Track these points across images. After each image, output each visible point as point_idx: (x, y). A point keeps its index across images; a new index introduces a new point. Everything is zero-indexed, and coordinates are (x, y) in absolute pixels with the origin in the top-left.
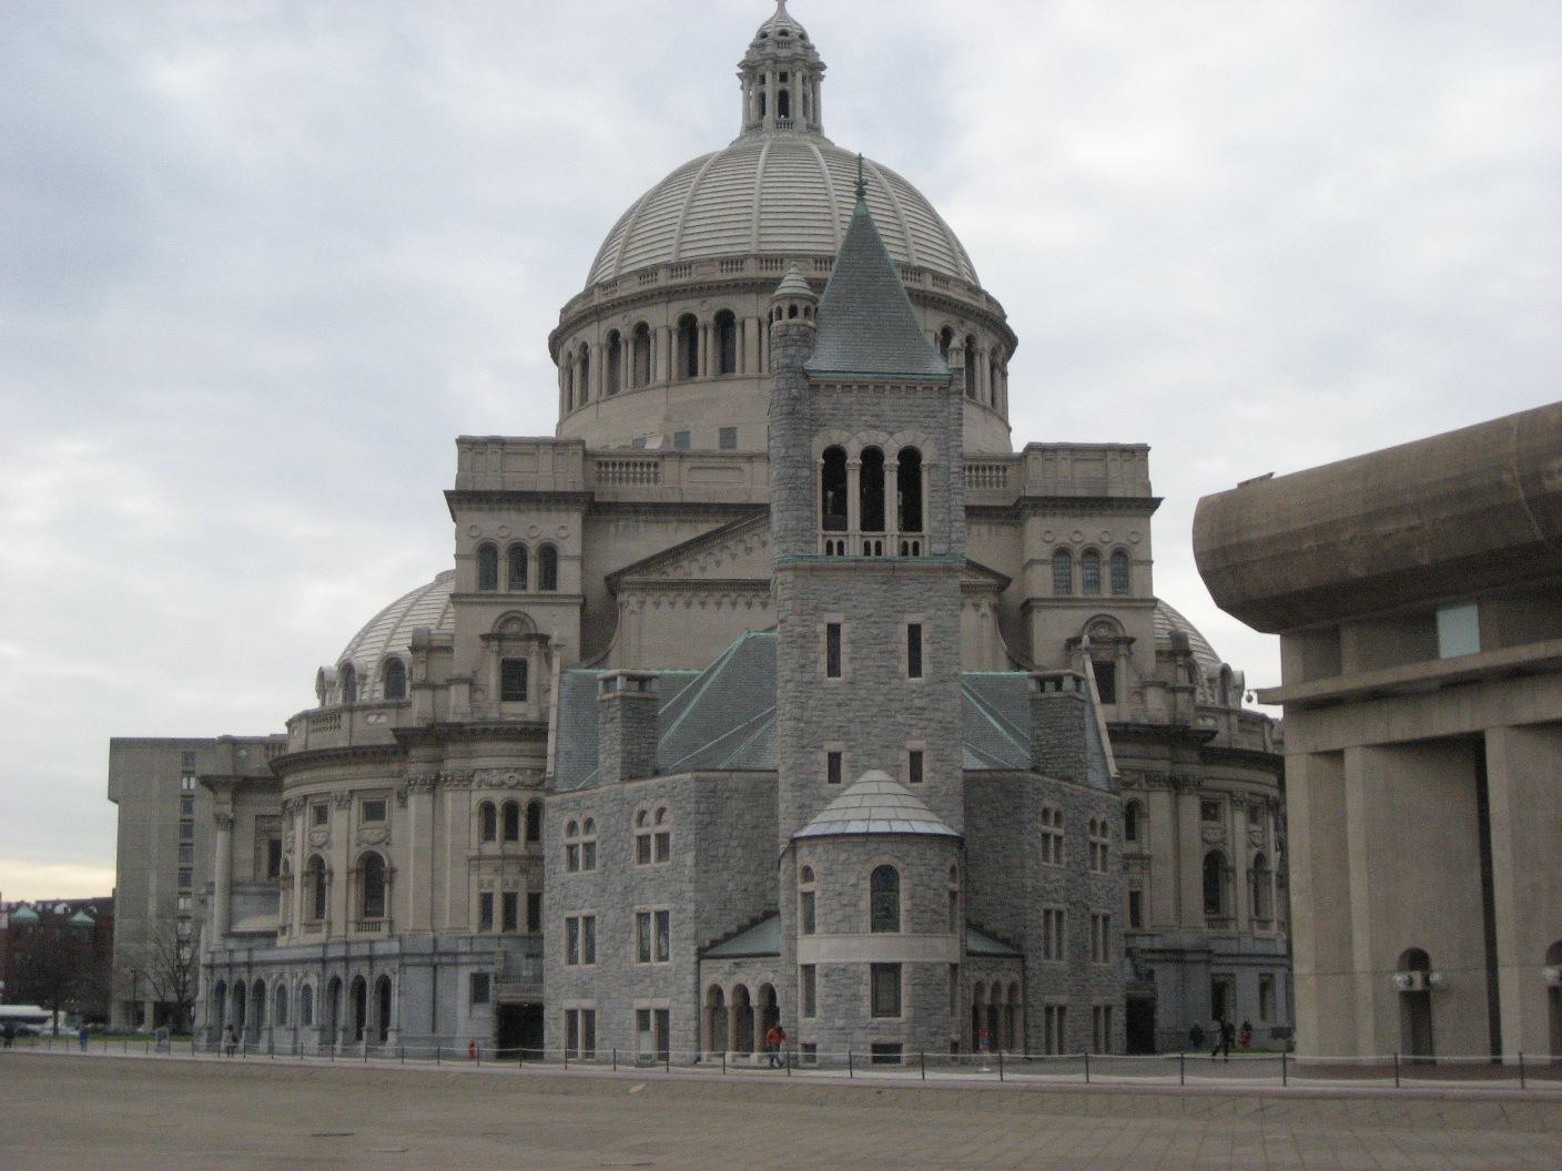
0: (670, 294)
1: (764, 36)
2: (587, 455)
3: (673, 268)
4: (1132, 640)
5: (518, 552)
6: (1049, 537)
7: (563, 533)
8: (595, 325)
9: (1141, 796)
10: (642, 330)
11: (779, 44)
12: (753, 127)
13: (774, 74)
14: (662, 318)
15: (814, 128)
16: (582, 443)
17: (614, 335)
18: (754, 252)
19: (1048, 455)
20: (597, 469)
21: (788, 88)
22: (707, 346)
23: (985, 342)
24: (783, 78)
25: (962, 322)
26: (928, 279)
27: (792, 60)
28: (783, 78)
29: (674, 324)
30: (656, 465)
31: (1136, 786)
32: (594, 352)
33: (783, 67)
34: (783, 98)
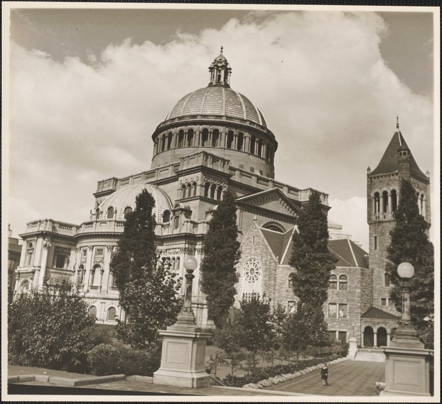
0: (177, 125)
1: (215, 60)
3: (180, 118)
12: (211, 85)
15: (227, 86)
17: (164, 135)
18: (201, 114)
22: (186, 137)
26: (248, 123)
27: (222, 67)
28: (220, 72)
32: (160, 140)
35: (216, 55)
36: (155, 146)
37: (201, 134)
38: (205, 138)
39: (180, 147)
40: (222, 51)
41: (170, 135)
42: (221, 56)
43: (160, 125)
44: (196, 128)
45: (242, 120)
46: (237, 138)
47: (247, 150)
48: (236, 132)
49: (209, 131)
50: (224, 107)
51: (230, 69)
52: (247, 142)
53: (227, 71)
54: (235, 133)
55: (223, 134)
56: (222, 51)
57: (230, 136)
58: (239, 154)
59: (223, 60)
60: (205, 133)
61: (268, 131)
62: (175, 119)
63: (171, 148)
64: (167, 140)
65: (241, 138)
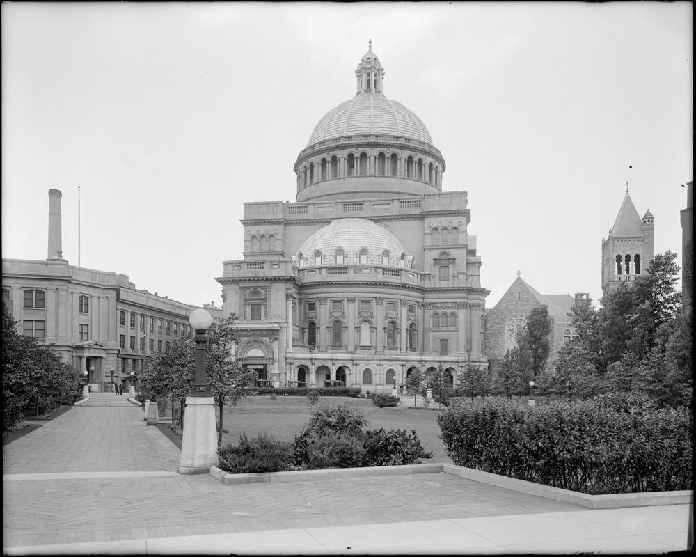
0: (318, 152)
1: (363, 60)
2: (284, 205)
4: (455, 259)
5: (263, 236)
6: (430, 225)
9: (456, 311)
10: (312, 164)
12: (359, 93)
14: (316, 160)
15: (380, 92)
16: (281, 202)
17: (305, 167)
19: (459, 195)
22: (329, 167)
23: (427, 160)
27: (371, 68)
28: (369, 75)
29: (320, 162)
34: (369, 81)
35: (364, 52)
38: (351, 166)
39: (324, 179)
40: (370, 47)
42: (370, 50)
43: (300, 155)
44: (337, 153)
46: (390, 160)
47: (403, 175)
48: (388, 155)
49: (355, 157)
50: (372, 126)
51: (383, 70)
52: (403, 165)
53: (380, 72)
54: (387, 155)
55: (373, 158)
56: (370, 47)
57: (382, 155)
58: (393, 180)
59: (372, 58)
60: (351, 157)
61: (430, 146)
62: (315, 145)
63: (316, 179)
64: (309, 172)
65: (394, 156)
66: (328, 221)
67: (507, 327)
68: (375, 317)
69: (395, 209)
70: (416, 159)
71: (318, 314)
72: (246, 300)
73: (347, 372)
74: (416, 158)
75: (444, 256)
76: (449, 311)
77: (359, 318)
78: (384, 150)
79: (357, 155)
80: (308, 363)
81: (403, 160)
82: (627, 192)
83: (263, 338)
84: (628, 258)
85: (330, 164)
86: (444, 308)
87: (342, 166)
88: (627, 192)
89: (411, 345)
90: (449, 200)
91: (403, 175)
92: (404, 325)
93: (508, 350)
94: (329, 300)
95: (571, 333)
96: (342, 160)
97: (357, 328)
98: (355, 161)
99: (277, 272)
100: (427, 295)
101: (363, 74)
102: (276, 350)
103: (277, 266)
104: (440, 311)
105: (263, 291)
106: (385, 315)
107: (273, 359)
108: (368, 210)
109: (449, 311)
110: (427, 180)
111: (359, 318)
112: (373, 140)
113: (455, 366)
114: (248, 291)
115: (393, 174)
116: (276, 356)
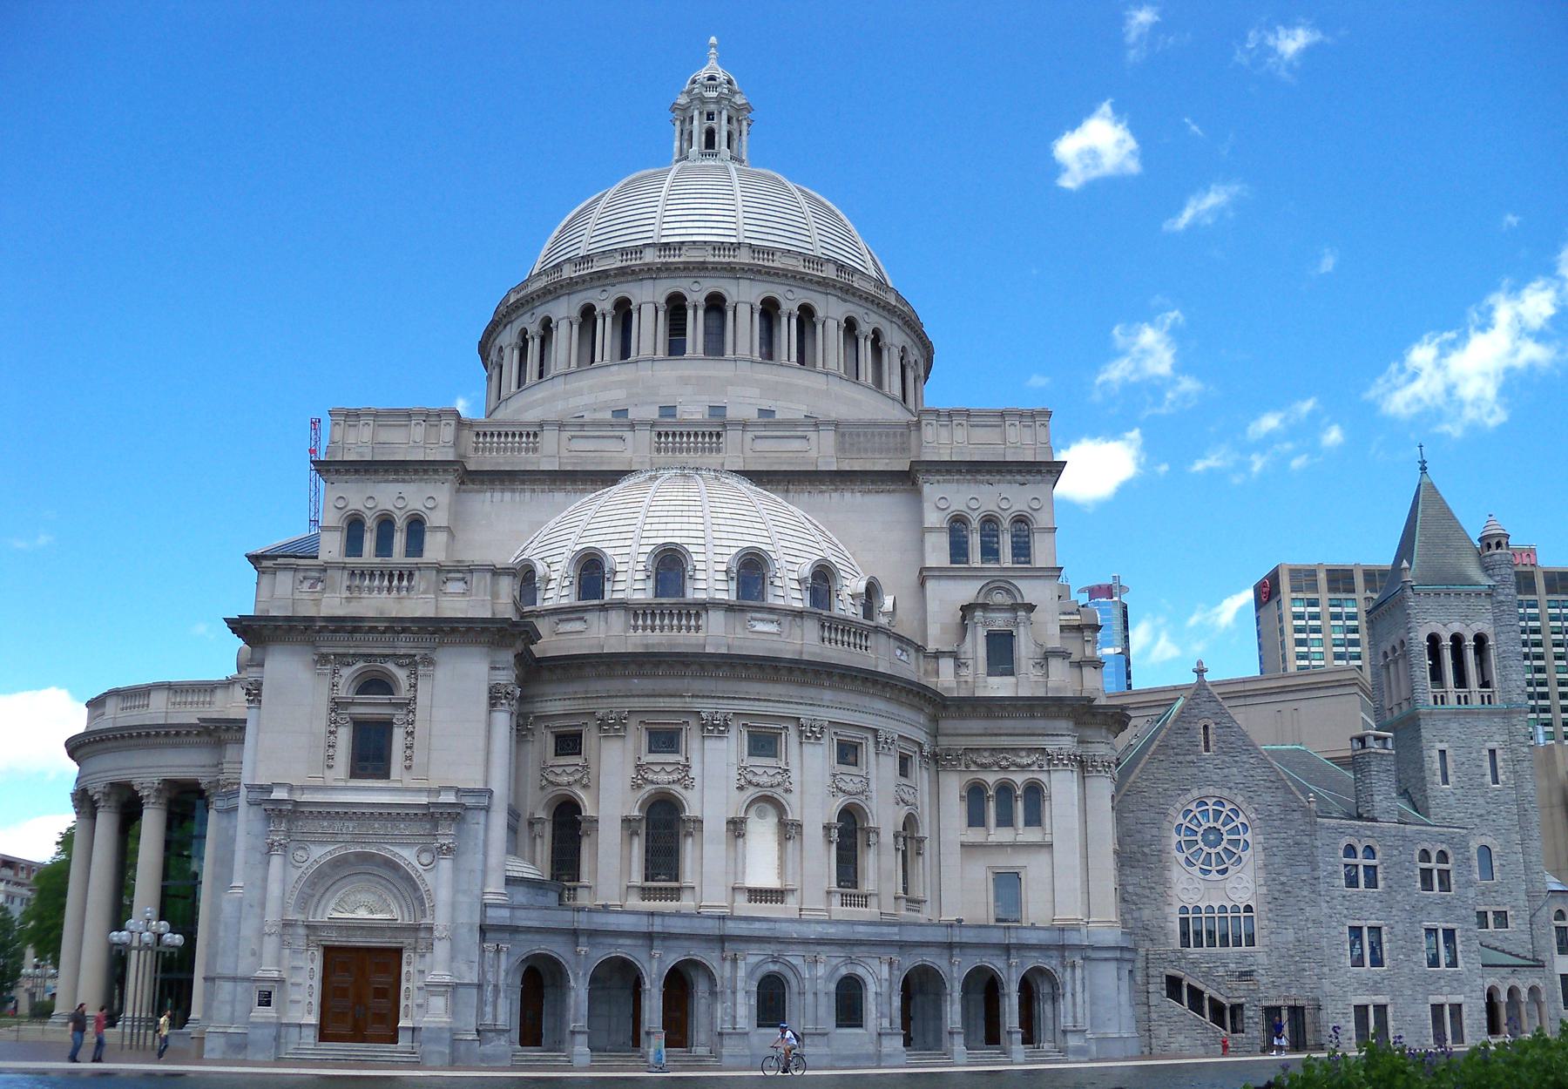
0: (572, 285)
6: (943, 504)
7: (430, 504)
8: (509, 327)
9: (1043, 777)
11: (707, 88)
13: (701, 113)
14: (564, 311)
16: (458, 415)
17: (524, 332)
20: (475, 439)
21: (716, 126)
22: (606, 332)
23: (895, 337)
24: (710, 116)
25: (866, 313)
27: (718, 100)
28: (710, 116)
29: (575, 313)
30: (535, 435)
31: (1035, 768)
32: (507, 352)
33: (712, 107)
34: (710, 135)
36: (489, 378)
37: (661, 314)
41: (547, 326)
45: (808, 259)
48: (790, 303)
52: (830, 340)
55: (743, 311)
57: (769, 310)
60: (676, 308)
66: (610, 478)
67: (1175, 838)
68: (795, 788)
69: (822, 452)
70: (865, 328)
71: (593, 771)
72: (337, 705)
73: (701, 988)
74: (868, 322)
75: (999, 598)
76: (1019, 779)
77: (741, 788)
78: (777, 291)
79: (696, 293)
80: (556, 948)
81: (832, 325)
82: (1423, 469)
83: (397, 850)
84: (1457, 640)
85: (609, 320)
86: (1005, 769)
87: (649, 329)
88: (1423, 469)
89: (905, 890)
90: (998, 429)
91: (832, 364)
92: (884, 817)
93: (1184, 909)
94: (633, 723)
95: (1360, 850)
96: (648, 312)
97: (736, 827)
98: (690, 313)
99: (458, 603)
100: (947, 725)
101: (696, 113)
102: (443, 895)
103: (457, 587)
104: (991, 779)
105: (401, 675)
106: (829, 781)
107: (430, 929)
108: (738, 450)
109: (1019, 779)
110: (897, 392)
111: (741, 788)
112: (744, 257)
113: (1051, 963)
114: (347, 672)
115: (801, 359)
116: (441, 919)
